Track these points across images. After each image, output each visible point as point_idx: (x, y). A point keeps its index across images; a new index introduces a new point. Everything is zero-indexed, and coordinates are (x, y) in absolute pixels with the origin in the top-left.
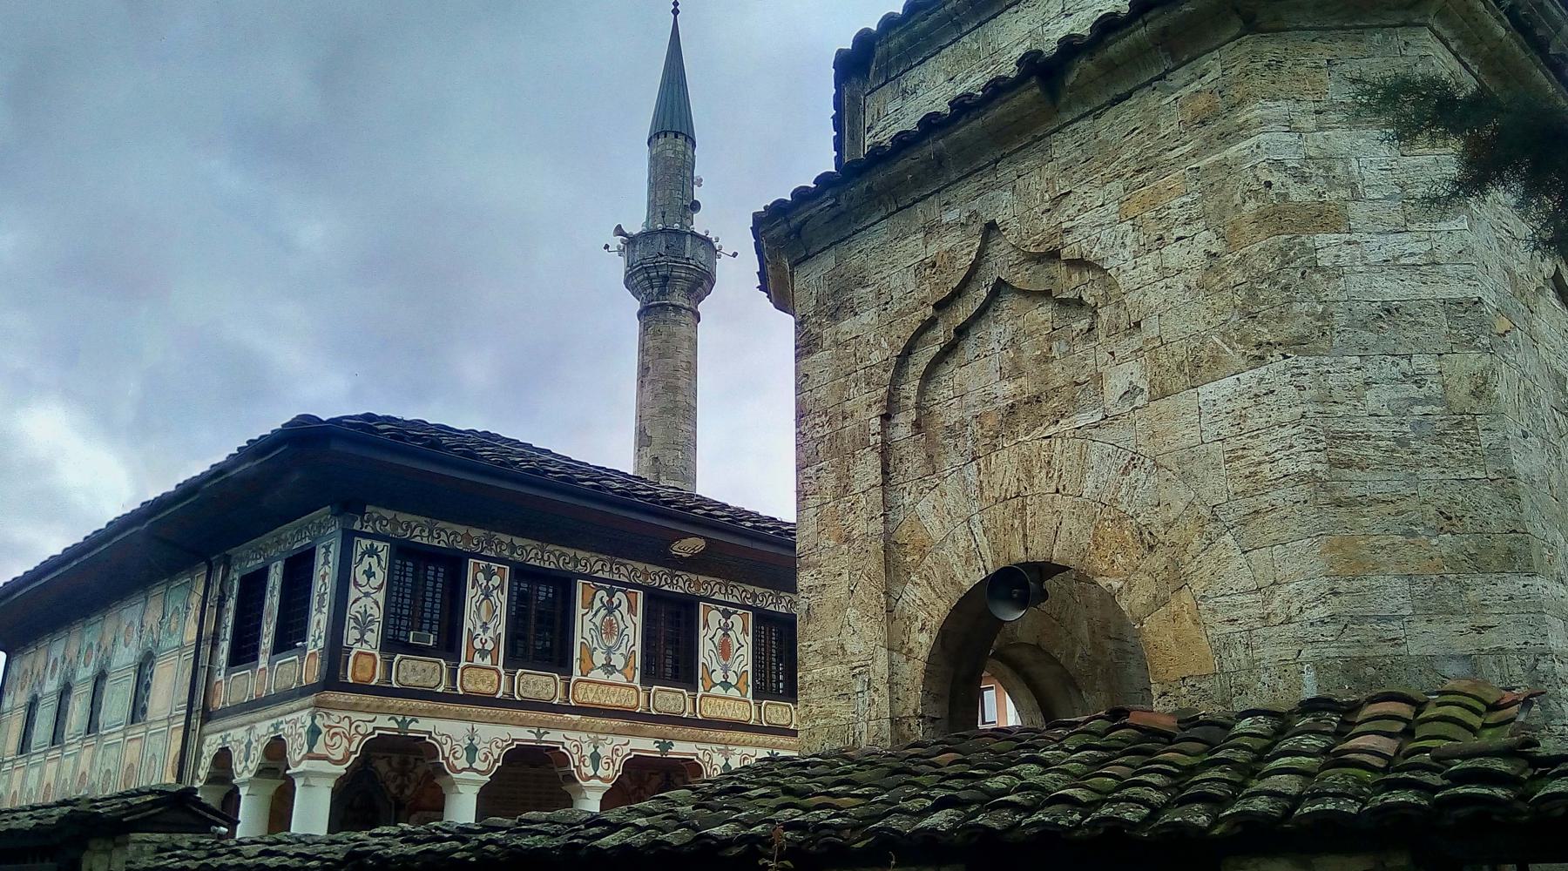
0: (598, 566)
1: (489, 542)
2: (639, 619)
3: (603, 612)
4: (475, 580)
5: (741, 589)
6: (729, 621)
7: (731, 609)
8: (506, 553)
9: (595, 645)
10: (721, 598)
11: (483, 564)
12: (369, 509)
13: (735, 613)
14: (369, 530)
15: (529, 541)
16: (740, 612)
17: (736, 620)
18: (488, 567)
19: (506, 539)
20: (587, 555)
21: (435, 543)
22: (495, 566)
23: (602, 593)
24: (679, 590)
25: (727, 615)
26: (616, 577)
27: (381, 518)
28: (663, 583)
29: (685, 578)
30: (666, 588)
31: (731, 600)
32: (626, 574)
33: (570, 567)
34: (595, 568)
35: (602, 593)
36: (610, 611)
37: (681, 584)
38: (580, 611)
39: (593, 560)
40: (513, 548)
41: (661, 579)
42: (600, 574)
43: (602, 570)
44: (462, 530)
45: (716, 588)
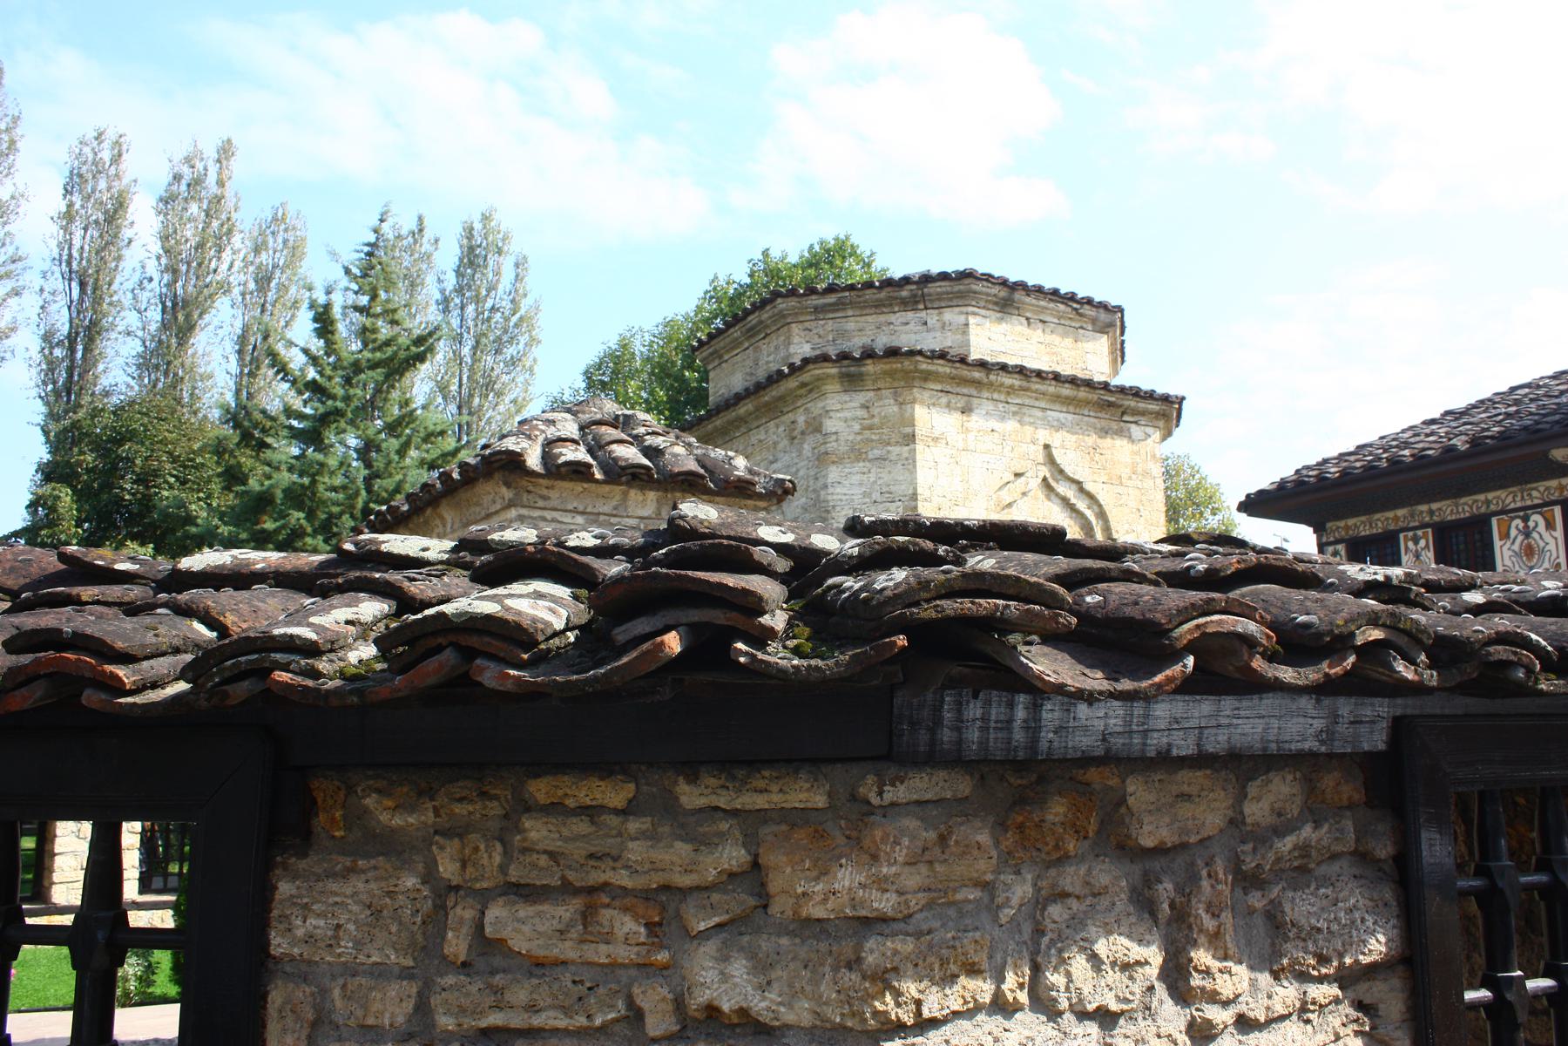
0: (1510, 498)
1: (1412, 516)
2: (1559, 533)
3: (1520, 538)
4: (1407, 548)
8: (1427, 519)
9: (1517, 568)
11: (1410, 534)
12: (1329, 525)
14: (1332, 539)
15: (1444, 503)
18: (1415, 535)
19: (1424, 508)
20: (1498, 493)
21: (1375, 531)
22: (1420, 533)
23: (1518, 522)
26: (1529, 503)
27: (1338, 528)
33: (1483, 510)
34: (1507, 502)
35: (1518, 522)
36: (1527, 534)
38: (1497, 543)
39: (1503, 496)
40: (1431, 513)
42: (1512, 506)
43: (1514, 501)
44: (1390, 514)
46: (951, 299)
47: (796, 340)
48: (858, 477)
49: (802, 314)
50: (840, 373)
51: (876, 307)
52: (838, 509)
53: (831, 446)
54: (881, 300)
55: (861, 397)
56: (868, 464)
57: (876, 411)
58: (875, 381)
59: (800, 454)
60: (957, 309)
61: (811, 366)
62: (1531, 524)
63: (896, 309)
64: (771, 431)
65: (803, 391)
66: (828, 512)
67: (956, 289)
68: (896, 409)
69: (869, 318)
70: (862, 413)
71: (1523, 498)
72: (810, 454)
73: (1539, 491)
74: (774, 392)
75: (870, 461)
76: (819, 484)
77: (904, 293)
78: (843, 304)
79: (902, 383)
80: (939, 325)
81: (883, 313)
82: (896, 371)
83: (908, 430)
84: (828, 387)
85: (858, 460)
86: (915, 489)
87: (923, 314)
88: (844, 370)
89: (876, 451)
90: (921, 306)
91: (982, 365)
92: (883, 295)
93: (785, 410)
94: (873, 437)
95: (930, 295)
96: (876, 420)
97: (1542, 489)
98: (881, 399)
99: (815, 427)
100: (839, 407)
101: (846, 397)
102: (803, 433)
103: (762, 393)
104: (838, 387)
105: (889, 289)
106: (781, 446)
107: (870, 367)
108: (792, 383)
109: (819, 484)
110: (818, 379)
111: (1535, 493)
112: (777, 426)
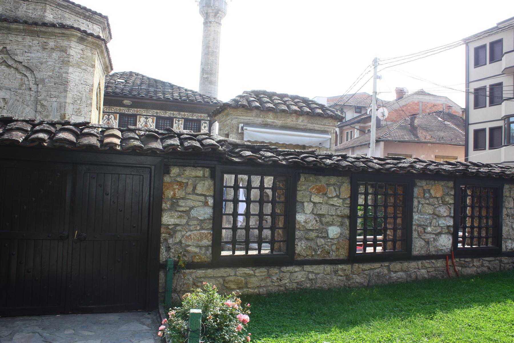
2: (117, 121)
3: (106, 120)
5: (152, 111)
6: (147, 120)
7: (148, 117)
10: (145, 114)
13: (150, 118)
16: (152, 117)
17: (150, 120)
23: (107, 115)
24: (131, 113)
25: (147, 118)
26: (110, 111)
28: (126, 111)
29: (133, 110)
30: (127, 113)
31: (148, 114)
32: (114, 110)
36: (109, 120)
37: (131, 111)
41: (125, 111)
45: (144, 112)
46: (97, 22)
47: (48, 11)
48: (78, 73)
49: (53, 3)
50: (81, 37)
51: (76, 13)
52: (71, 82)
53: (71, 60)
54: (79, 12)
55: (81, 47)
56: (81, 70)
57: (85, 53)
58: (87, 43)
59: (50, 56)
60: (99, 26)
61: (73, 30)
62: (110, 117)
63: (82, 17)
64: (27, 40)
65: (59, 35)
66: (68, 82)
67: (101, 20)
68: (91, 55)
69: (73, 16)
70: (81, 52)
71: (109, 109)
72: (57, 58)
73: (114, 109)
74: (43, 29)
75: (82, 69)
76: (65, 70)
77: (87, 14)
78: (68, 7)
79: (94, 47)
80: (92, 29)
81: (77, 16)
82: (95, 43)
83: (93, 63)
84: (73, 39)
85: (78, 67)
86: (93, 83)
87: (88, 23)
88: (82, 36)
89: (84, 67)
90: (88, 20)
91: (107, 49)
92: (81, 11)
93: (41, 36)
94: (83, 61)
95: (93, 18)
96: (85, 56)
97: (115, 109)
98: (87, 50)
99: (64, 50)
100: (74, 47)
101: (77, 44)
102: (51, 49)
103: (35, 26)
104: (76, 40)
105: (84, 10)
106: (35, 48)
107: (90, 39)
108: (57, 31)
109: (64, 70)
110: (71, 35)
111: (113, 109)
112: (33, 40)
